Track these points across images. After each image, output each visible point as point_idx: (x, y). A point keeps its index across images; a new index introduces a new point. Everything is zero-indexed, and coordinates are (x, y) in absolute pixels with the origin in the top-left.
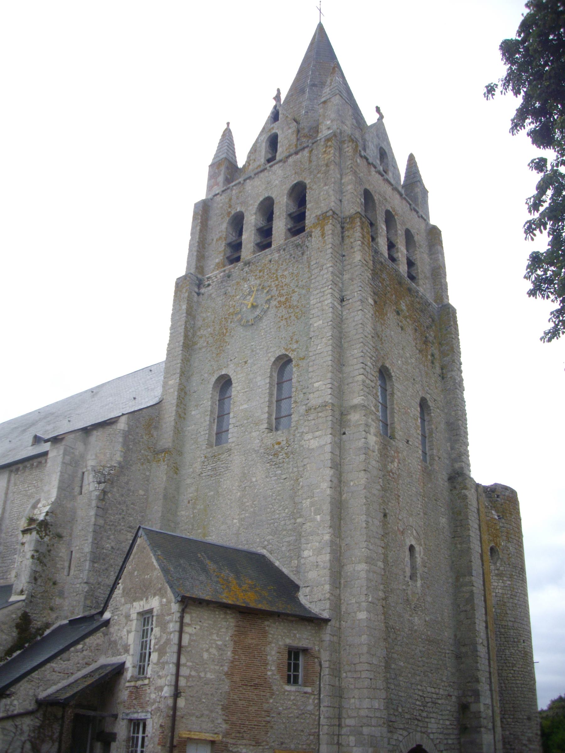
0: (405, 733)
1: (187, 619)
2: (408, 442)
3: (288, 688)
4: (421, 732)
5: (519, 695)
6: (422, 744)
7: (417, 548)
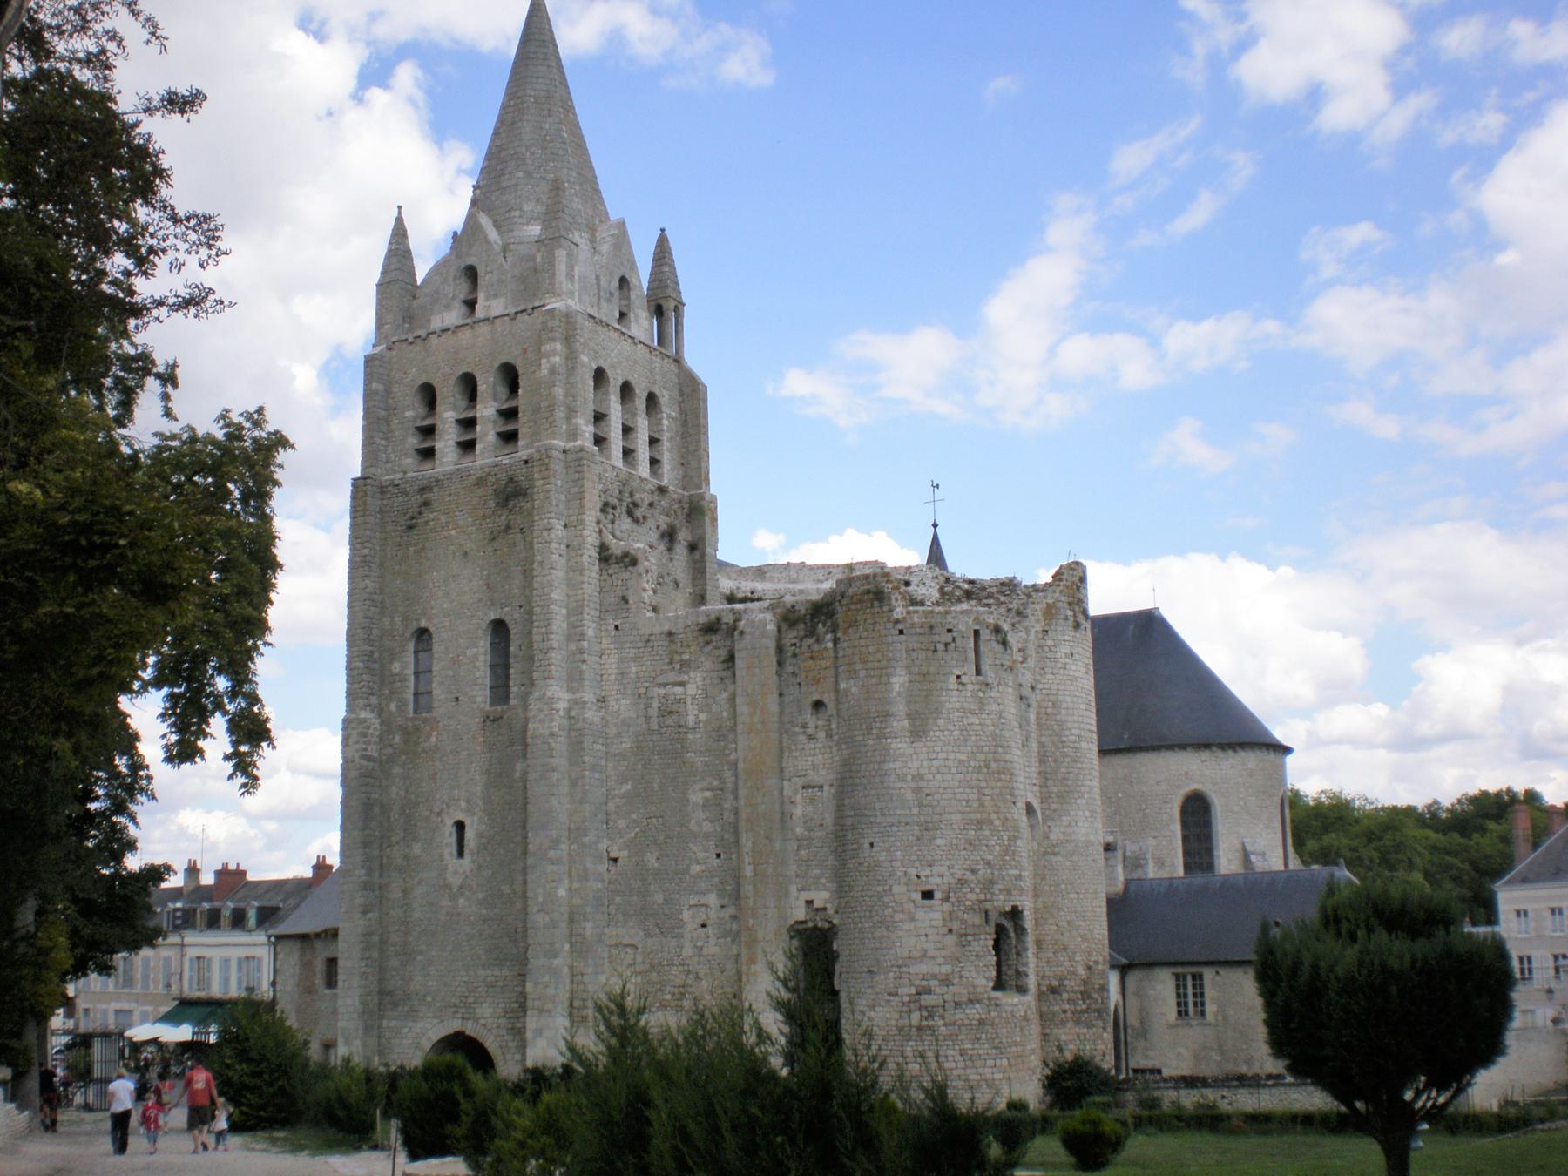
0: (435, 1021)
1: (278, 948)
2: (457, 698)
3: (327, 991)
4: (463, 1019)
5: (857, 935)
6: (463, 1029)
7: (468, 822)
